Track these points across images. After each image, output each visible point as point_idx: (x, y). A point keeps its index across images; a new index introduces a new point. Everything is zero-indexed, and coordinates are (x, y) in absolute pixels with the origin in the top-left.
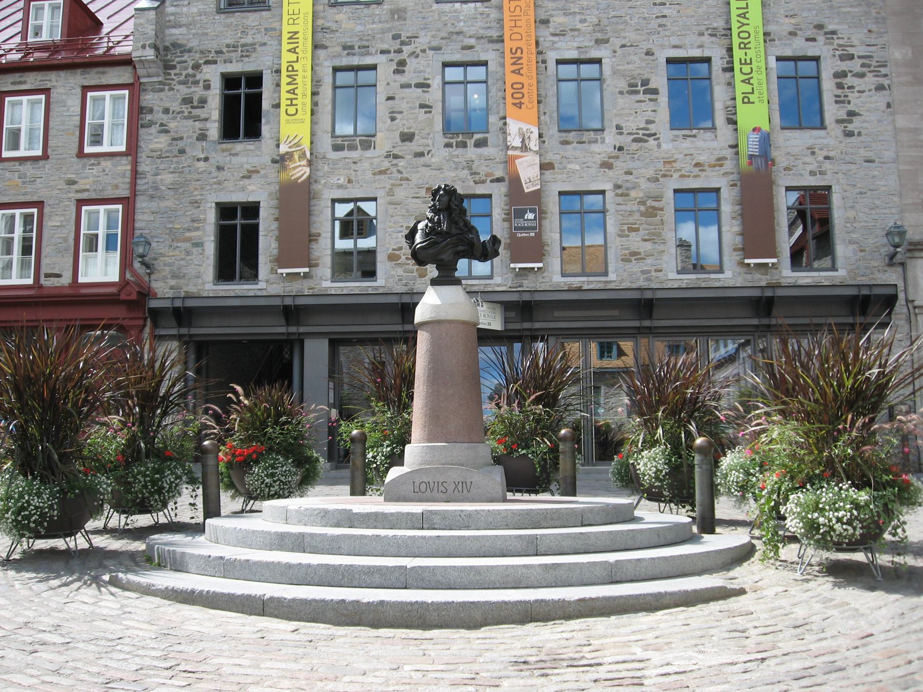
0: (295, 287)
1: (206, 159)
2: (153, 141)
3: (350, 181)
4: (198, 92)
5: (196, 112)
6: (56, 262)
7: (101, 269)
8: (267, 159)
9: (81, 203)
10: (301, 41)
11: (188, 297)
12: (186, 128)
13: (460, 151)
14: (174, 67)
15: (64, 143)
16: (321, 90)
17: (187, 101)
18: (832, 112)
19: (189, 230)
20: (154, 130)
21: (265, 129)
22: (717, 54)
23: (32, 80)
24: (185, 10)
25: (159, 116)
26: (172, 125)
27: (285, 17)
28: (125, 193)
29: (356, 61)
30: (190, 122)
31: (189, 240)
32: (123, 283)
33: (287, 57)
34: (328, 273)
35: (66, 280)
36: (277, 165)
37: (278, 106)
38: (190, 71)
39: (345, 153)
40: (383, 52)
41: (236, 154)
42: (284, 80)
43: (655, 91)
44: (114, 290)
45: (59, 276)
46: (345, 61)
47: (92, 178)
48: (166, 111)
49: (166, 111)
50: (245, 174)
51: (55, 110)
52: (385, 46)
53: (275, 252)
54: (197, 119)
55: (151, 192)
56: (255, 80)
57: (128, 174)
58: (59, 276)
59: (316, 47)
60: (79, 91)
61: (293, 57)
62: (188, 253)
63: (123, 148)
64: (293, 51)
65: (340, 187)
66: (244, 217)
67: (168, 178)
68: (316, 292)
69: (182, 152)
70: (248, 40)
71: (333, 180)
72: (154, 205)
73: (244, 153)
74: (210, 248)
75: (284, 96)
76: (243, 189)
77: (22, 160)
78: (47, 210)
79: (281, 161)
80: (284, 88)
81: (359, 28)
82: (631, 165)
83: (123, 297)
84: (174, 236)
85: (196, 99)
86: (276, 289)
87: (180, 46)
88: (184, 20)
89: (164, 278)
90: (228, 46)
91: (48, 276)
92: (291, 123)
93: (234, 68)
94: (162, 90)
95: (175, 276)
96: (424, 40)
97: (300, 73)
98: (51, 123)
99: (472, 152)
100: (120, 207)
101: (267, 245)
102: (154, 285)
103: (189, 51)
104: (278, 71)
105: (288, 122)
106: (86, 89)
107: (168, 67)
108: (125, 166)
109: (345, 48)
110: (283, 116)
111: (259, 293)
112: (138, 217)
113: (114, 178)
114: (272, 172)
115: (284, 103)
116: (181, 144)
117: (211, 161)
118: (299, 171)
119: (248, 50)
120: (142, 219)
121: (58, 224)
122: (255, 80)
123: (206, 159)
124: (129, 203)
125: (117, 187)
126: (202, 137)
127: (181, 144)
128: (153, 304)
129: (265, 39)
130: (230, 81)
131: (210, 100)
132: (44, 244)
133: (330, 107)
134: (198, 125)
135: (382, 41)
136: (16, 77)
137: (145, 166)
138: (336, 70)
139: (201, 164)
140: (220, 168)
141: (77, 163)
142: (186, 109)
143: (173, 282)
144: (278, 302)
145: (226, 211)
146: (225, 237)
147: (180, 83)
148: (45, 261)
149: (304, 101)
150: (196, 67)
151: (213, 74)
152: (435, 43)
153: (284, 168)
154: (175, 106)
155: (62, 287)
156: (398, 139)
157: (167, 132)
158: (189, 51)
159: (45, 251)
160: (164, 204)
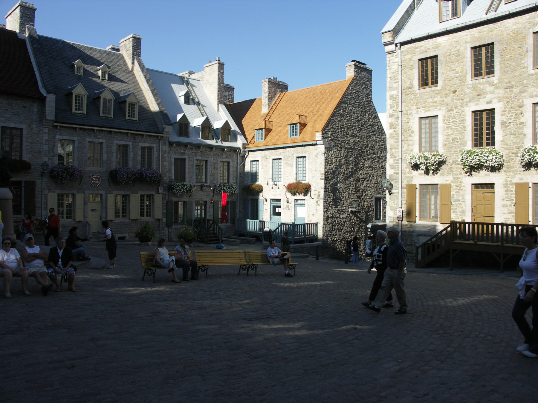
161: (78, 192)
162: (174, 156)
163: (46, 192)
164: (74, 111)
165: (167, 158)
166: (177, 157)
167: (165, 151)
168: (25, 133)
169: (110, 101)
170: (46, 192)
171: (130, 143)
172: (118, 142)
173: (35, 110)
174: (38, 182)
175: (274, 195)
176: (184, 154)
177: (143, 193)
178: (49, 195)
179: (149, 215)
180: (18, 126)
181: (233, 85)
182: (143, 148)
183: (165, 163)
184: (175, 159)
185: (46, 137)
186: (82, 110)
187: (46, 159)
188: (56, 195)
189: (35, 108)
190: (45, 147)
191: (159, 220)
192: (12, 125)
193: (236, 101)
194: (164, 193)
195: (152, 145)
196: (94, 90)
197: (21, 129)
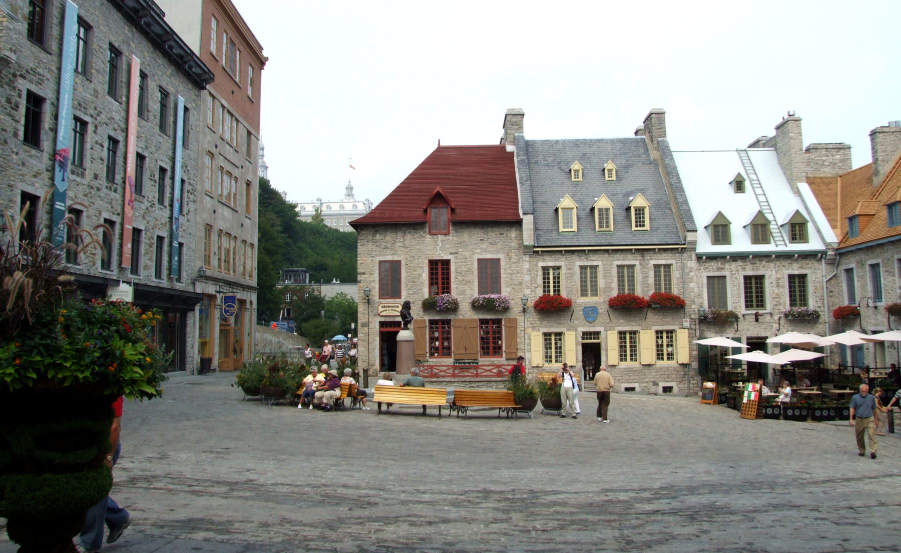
8: (44, 166)
13: (109, 192)
18: (185, 211)
22: (168, 168)
40: (92, 116)
41: (31, 156)
43: (155, 181)
52: (92, 113)
82: (149, 219)
85: (13, 101)
93: (34, 88)
96: (103, 118)
99: (113, 195)
123: (17, 154)
126: (16, 135)
152: (107, 120)
156: (93, 176)
161: (568, 330)
162: (705, 274)
163: (529, 330)
164: (561, 229)
165: (695, 278)
166: (711, 274)
167: (691, 268)
168: (502, 263)
169: (607, 210)
170: (529, 330)
171: (637, 263)
172: (620, 263)
173: (513, 236)
174: (520, 319)
175: (875, 325)
176: (722, 269)
177: (660, 328)
178: (533, 334)
179: (670, 356)
180: (495, 256)
181: (847, 142)
182: (657, 267)
183: (692, 285)
184: (708, 277)
185: (527, 266)
186: (571, 227)
187: (527, 292)
188: (540, 334)
189: (513, 233)
190: (527, 278)
191: (684, 365)
192: (489, 256)
193: (854, 167)
194: (693, 327)
195: (669, 262)
196: (594, 197)
197: (499, 260)
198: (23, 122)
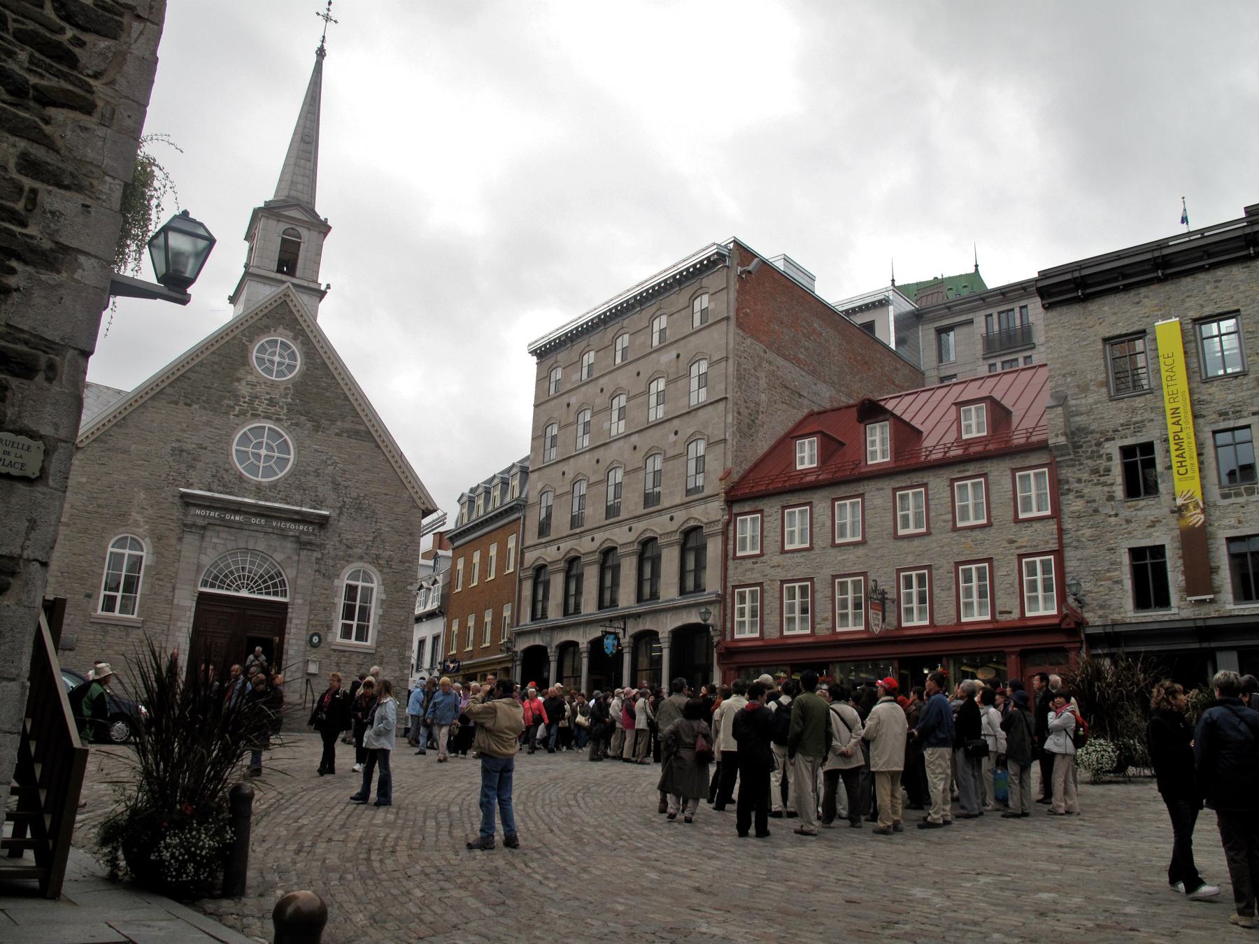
0: (1203, 612)
1: (1116, 515)
2: (1073, 505)
3: (1240, 522)
4: (1103, 463)
5: (1102, 479)
6: (1007, 602)
7: (1044, 609)
8: (1166, 511)
9: (1021, 556)
10: (1182, 414)
11: (1115, 624)
12: (1097, 492)
14: (1081, 446)
15: (1003, 513)
16: (1205, 451)
17: (1095, 471)
19: (1109, 571)
20: (1071, 496)
21: (1161, 487)
23: (972, 469)
24: (1083, 401)
25: (1076, 486)
26: (1086, 491)
27: (1166, 398)
28: (1055, 547)
29: (1231, 424)
30: (1099, 488)
31: (1110, 579)
32: (1062, 617)
33: (1172, 429)
34: (1230, 597)
35: (1016, 615)
36: (1176, 515)
37: (1170, 468)
38: (1095, 448)
39: (1233, 500)
41: (1140, 509)
42: (1173, 447)
44: (1056, 621)
45: (1010, 613)
46: (1222, 425)
47: (1026, 537)
48: (1079, 481)
49: (1079, 481)
50: (1151, 524)
51: (993, 489)
53: (1183, 584)
54: (1104, 484)
55: (1075, 544)
56: (1148, 448)
57: (1055, 531)
58: (1010, 613)
59: (1195, 417)
60: (1009, 472)
61: (1177, 428)
62: (1111, 589)
63: (1048, 513)
64: (1176, 423)
65: (1232, 527)
66: (1153, 557)
67: (1088, 532)
68: (1222, 613)
69: (1096, 511)
70: (1138, 418)
71: (1225, 522)
72: (1079, 553)
73: (1147, 508)
74: (1128, 584)
75: (1174, 460)
76: (1150, 535)
77: (972, 528)
78: (995, 563)
79: (1180, 511)
80: (1173, 453)
81: (1231, 397)
83: (1064, 626)
84: (1098, 576)
86: (1187, 613)
87: (1083, 429)
88: (1083, 409)
89: (1093, 610)
90: (1122, 425)
91: (1001, 613)
92: (1184, 481)
94: (1073, 466)
95: (1102, 607)
97: (1185, 440)
98: (992, 499)
100: (1052, 557)
101: (1175, 579)
102: (1086, 615)
103: (1092, 432)
104: (1167, 440)
105: (1180, 480)
106: (1014, 471)
107: (1076, 446)
108: (1052, 526)
109: (1220, 415)
110: (1176, 476)
111: (1173, 618)
112: (1067, 564)
113: (1045, 535)
114: (1172, 521)
115: (1175, 465)
116: (1094, 505)
117: (1121, 516)
118: (1196, 518)
119: (1139, 427)
120: (1071, 565)
121: (1006, 572)
122: (1148, 448)
123: (1116, 515)
124: (1059, 554)
125: (1047, 542)
126: (1111, 498)
127: (1094, 505)
128: (1089, 631)
129: (1153, 416)
130: (1127, 452)
131: (1113, 468)
132: (996, 589)
133: (1214, 464)
134: (1106, 489)
135: (1252, 405)
136: (961, 467)
137: (1068, 524)
138: (1214, 432)
139: (1113, 519)
140: (1128, 521)
141: (1015, 528)
142: (1095, 478)
143: (1101, 612)
144: (1191, 624)
145: (1136, 553)
146: (1139, 575)
147: (1088, 458)
148: (998, 602)
149: (1192, 461)
150: (1099, 444)
151: (1113, 448)
153: (1182, 517)
154: (1085, 476)
155: (1014, 620)
157: (1082, 497)
158: (1092, 432)
159: (998, 594)
160: (1087, 553)
198: (1119, 480)
